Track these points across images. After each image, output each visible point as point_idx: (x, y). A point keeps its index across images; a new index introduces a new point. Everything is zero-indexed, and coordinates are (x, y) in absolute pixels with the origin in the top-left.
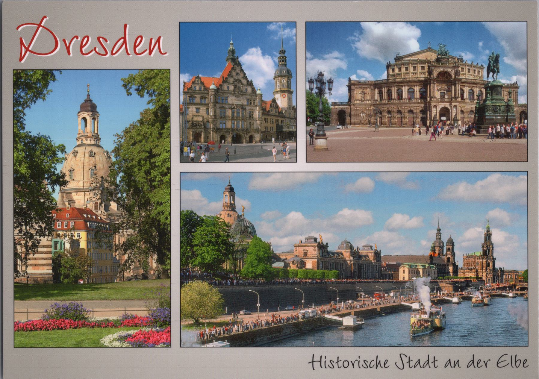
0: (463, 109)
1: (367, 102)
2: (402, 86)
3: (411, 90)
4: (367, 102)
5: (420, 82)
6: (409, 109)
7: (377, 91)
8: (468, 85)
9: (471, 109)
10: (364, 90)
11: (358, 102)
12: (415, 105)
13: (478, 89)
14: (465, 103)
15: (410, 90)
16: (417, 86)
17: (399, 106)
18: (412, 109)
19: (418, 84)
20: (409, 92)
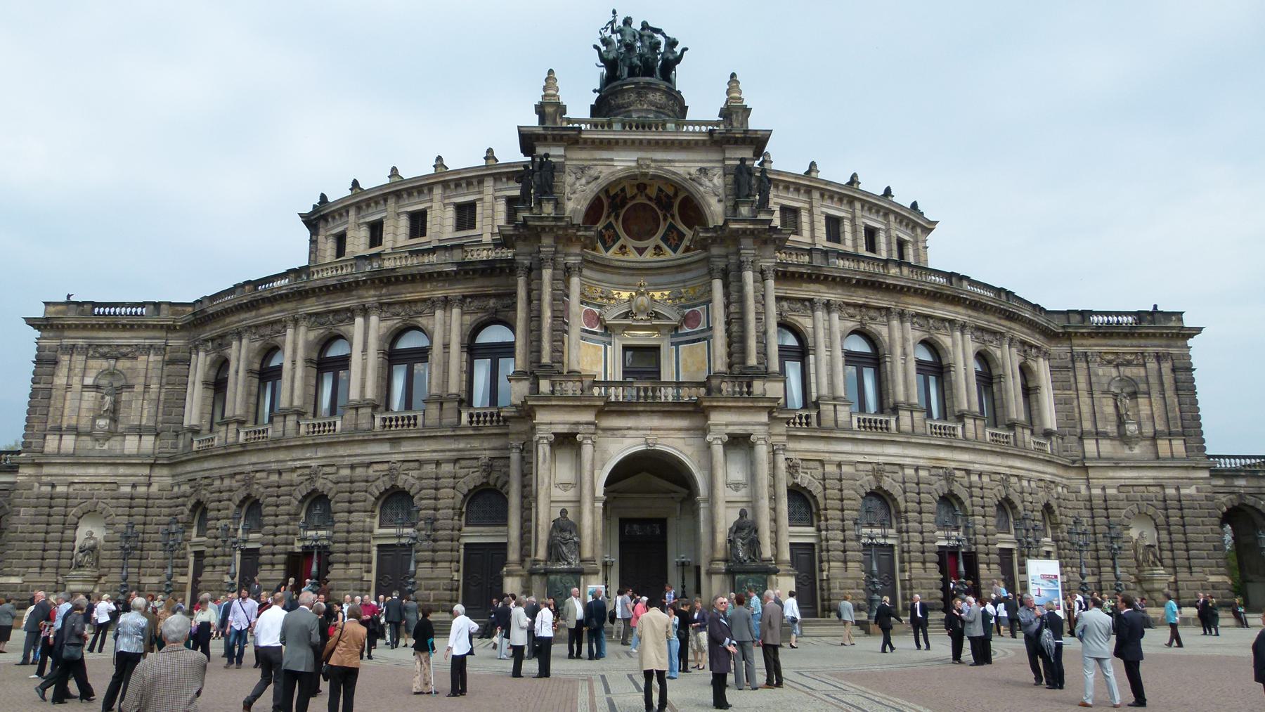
0: (804, 479)
1: (131, 444)
2: (350, 314)
3: (410, 342)
4: (131, 444)
5: (467, 271)
6: (383, 485)
7: (201, 363)
8: (834, 295)
9: (868, 482)
10: (123, 364)
11: (69, 442)
12: (427, 450)
13: (914, 335)
14: (826, 433)
15: (406, 343)
16: (446, 303)
17: (315, 458)
18: (407, 480)
19: (456, 291)
20: (392, 356)
